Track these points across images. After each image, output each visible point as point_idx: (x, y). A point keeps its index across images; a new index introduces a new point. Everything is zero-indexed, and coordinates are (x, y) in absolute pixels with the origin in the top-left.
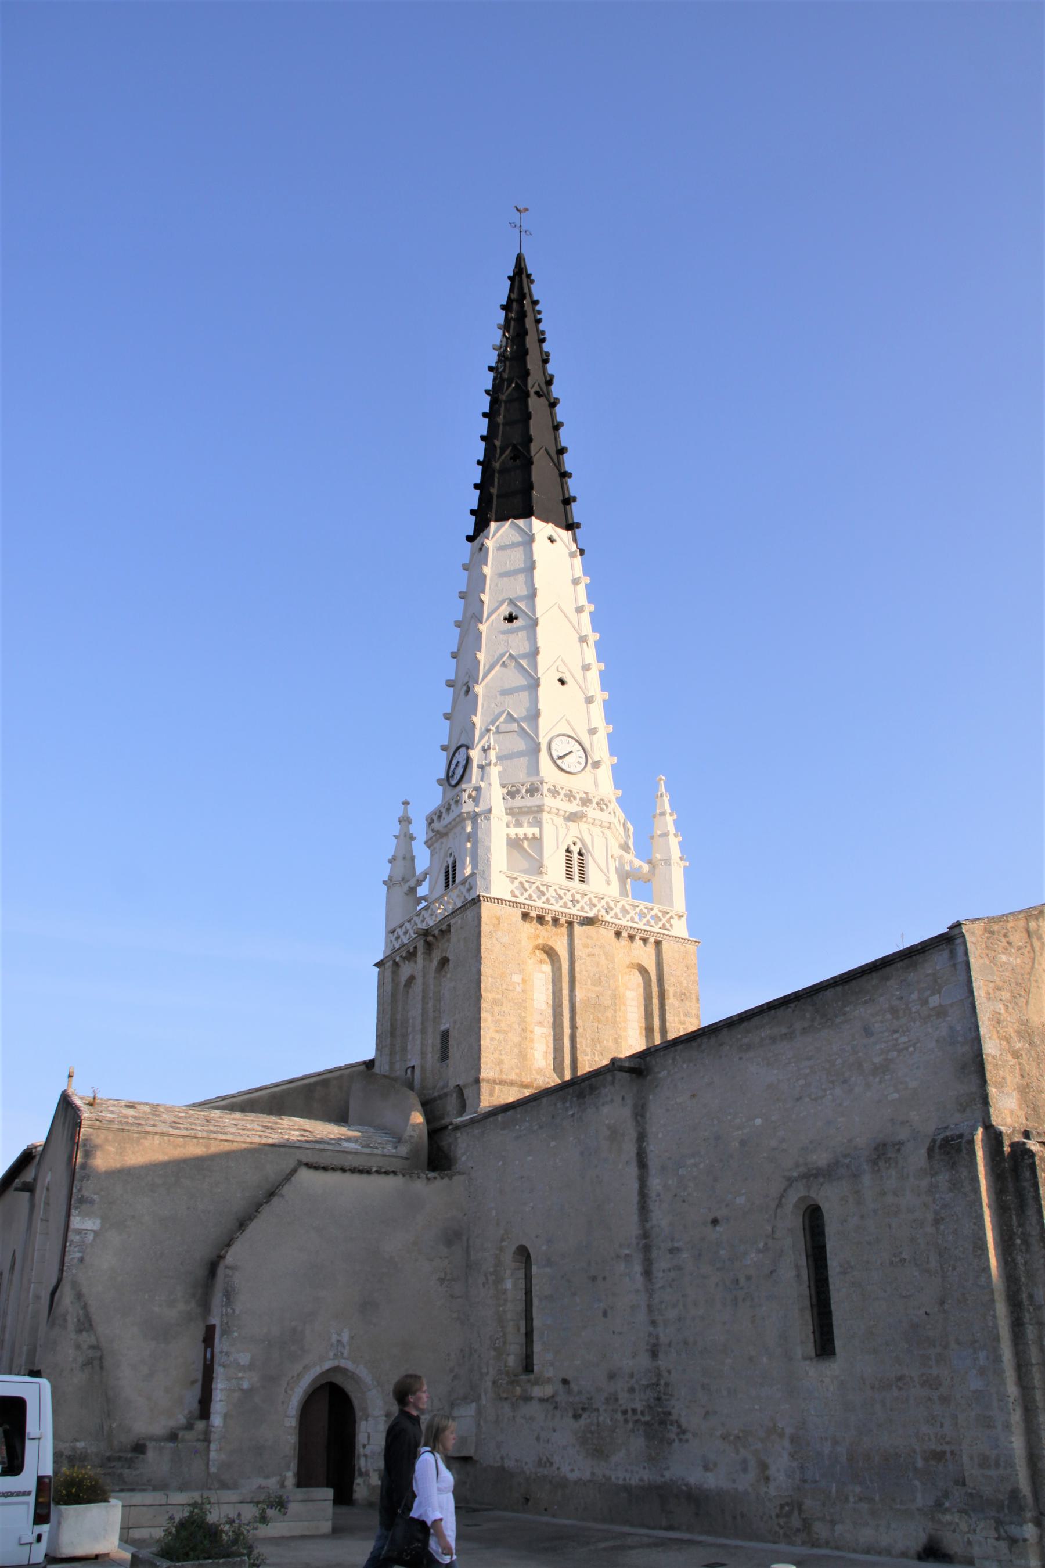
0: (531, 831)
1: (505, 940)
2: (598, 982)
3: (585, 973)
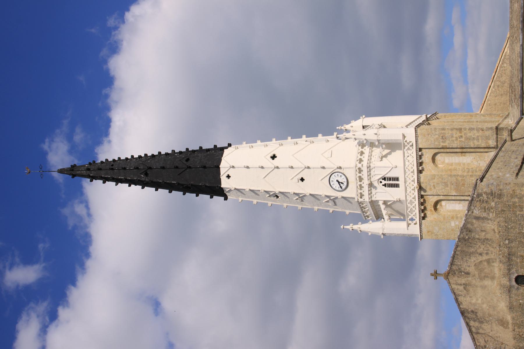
0: (383, 207)
1: (437, 228)
2: (446, 185)
3: (443, 190)
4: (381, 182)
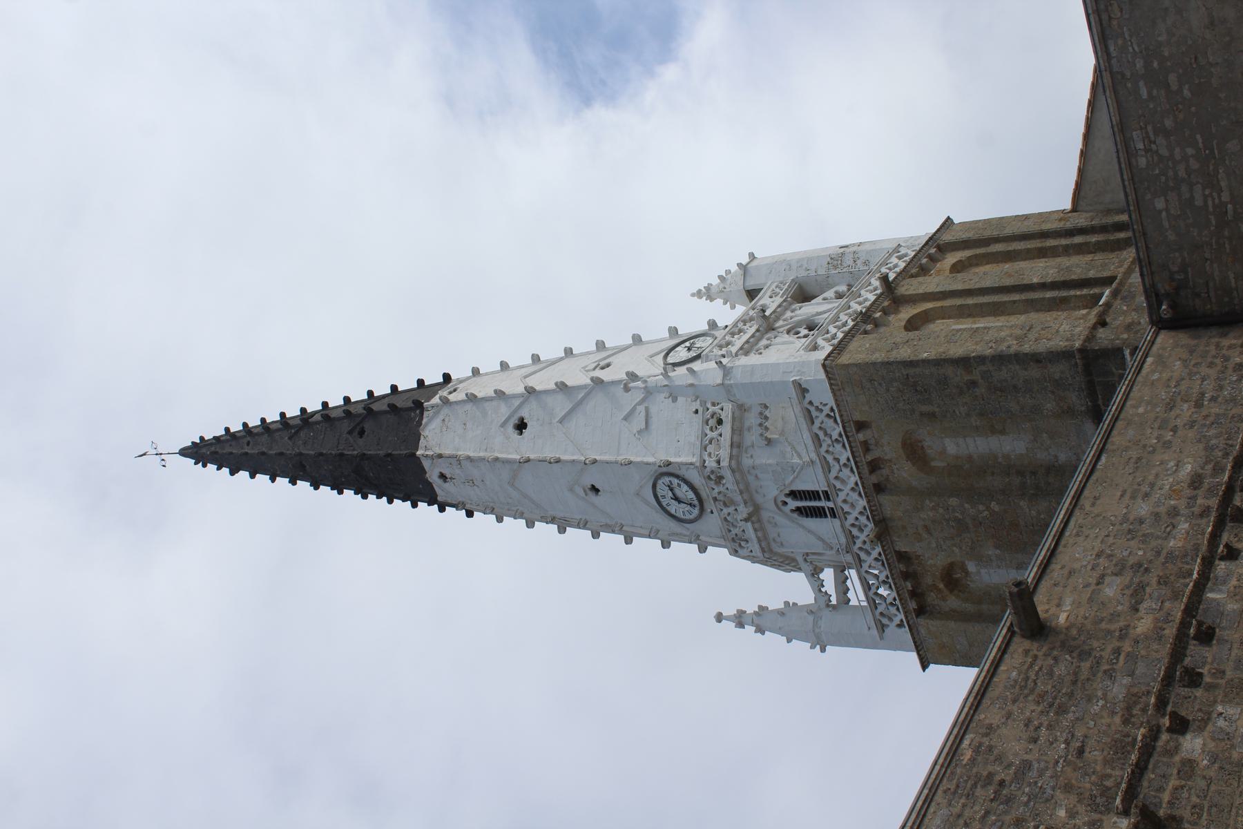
4: (785, 503)
